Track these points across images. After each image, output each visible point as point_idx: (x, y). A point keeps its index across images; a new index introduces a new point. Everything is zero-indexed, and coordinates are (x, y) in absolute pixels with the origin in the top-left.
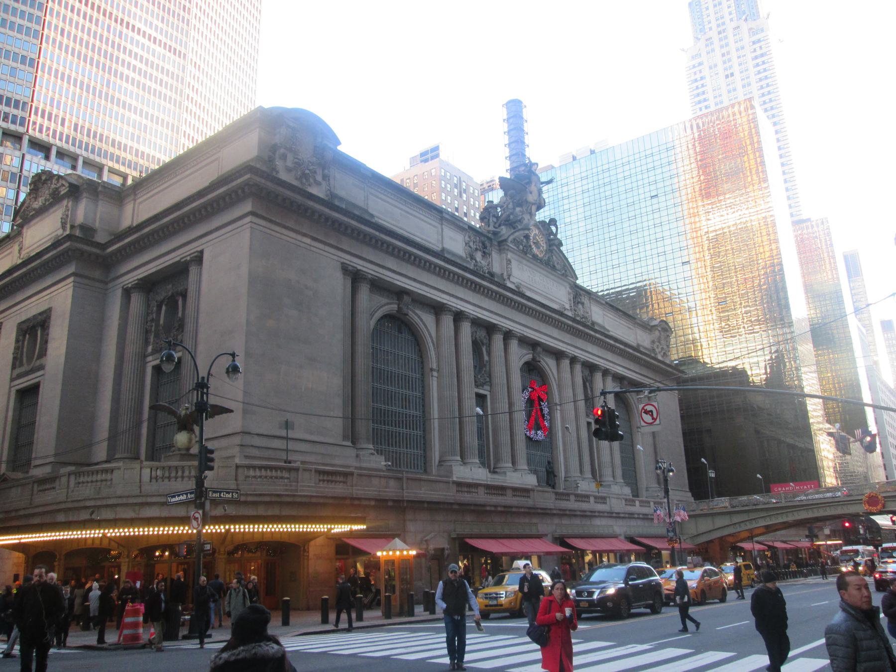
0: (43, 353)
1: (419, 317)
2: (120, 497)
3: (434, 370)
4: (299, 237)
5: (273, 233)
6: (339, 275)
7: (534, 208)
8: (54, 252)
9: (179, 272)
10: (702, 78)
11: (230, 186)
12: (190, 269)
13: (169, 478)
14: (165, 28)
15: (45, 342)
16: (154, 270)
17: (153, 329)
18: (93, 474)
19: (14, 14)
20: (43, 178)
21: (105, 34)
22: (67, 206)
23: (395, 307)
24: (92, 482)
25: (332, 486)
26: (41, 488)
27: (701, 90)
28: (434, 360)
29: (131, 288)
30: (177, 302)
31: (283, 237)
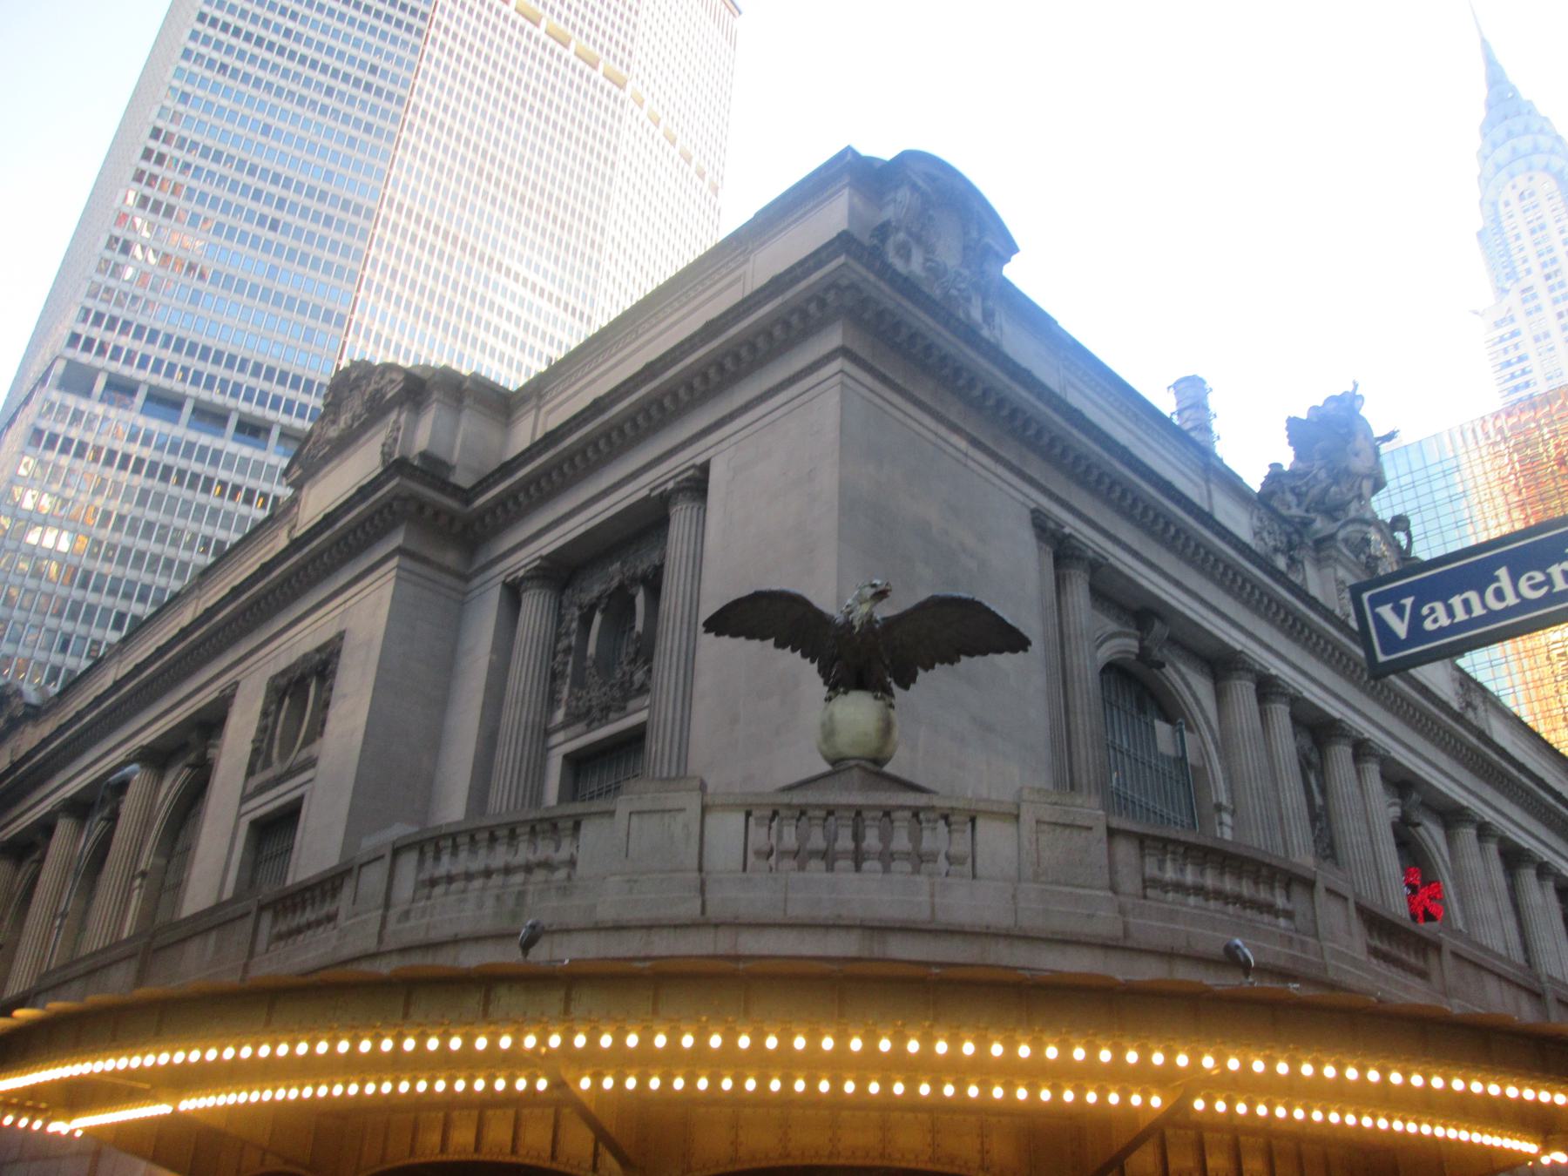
0: (318, 729)
1: (1183, 678)
2: (619, 928)
3: (1226, 809)
4: (943, 431)
5: (888, 407)
6: (1027, 535)
7: (1367, 486)
8: (362, 507)
9: (647, 523)
10: (1521, 359)
11: (789, 294)
12: (673, 511)
13: (828, 857)
14: (559, 273)
15: (324, 705)
16: (582, 529)
17: (569, 669)
18: (493, 839)
19: (321, 245)
20: (353, 376)
21: (462, 279)
22: (396, 422)
23: (1133, 645)
24: (488, 873)
25: (1395, 974)
26: (283, 927)
27: (1520, 380)
28: (1221, 785)
29: (523, 578)
30: (633, 598)
31: (909, 421)
